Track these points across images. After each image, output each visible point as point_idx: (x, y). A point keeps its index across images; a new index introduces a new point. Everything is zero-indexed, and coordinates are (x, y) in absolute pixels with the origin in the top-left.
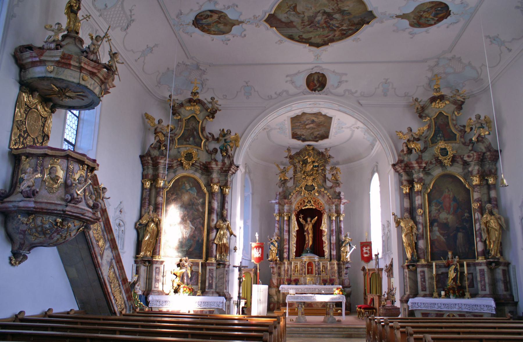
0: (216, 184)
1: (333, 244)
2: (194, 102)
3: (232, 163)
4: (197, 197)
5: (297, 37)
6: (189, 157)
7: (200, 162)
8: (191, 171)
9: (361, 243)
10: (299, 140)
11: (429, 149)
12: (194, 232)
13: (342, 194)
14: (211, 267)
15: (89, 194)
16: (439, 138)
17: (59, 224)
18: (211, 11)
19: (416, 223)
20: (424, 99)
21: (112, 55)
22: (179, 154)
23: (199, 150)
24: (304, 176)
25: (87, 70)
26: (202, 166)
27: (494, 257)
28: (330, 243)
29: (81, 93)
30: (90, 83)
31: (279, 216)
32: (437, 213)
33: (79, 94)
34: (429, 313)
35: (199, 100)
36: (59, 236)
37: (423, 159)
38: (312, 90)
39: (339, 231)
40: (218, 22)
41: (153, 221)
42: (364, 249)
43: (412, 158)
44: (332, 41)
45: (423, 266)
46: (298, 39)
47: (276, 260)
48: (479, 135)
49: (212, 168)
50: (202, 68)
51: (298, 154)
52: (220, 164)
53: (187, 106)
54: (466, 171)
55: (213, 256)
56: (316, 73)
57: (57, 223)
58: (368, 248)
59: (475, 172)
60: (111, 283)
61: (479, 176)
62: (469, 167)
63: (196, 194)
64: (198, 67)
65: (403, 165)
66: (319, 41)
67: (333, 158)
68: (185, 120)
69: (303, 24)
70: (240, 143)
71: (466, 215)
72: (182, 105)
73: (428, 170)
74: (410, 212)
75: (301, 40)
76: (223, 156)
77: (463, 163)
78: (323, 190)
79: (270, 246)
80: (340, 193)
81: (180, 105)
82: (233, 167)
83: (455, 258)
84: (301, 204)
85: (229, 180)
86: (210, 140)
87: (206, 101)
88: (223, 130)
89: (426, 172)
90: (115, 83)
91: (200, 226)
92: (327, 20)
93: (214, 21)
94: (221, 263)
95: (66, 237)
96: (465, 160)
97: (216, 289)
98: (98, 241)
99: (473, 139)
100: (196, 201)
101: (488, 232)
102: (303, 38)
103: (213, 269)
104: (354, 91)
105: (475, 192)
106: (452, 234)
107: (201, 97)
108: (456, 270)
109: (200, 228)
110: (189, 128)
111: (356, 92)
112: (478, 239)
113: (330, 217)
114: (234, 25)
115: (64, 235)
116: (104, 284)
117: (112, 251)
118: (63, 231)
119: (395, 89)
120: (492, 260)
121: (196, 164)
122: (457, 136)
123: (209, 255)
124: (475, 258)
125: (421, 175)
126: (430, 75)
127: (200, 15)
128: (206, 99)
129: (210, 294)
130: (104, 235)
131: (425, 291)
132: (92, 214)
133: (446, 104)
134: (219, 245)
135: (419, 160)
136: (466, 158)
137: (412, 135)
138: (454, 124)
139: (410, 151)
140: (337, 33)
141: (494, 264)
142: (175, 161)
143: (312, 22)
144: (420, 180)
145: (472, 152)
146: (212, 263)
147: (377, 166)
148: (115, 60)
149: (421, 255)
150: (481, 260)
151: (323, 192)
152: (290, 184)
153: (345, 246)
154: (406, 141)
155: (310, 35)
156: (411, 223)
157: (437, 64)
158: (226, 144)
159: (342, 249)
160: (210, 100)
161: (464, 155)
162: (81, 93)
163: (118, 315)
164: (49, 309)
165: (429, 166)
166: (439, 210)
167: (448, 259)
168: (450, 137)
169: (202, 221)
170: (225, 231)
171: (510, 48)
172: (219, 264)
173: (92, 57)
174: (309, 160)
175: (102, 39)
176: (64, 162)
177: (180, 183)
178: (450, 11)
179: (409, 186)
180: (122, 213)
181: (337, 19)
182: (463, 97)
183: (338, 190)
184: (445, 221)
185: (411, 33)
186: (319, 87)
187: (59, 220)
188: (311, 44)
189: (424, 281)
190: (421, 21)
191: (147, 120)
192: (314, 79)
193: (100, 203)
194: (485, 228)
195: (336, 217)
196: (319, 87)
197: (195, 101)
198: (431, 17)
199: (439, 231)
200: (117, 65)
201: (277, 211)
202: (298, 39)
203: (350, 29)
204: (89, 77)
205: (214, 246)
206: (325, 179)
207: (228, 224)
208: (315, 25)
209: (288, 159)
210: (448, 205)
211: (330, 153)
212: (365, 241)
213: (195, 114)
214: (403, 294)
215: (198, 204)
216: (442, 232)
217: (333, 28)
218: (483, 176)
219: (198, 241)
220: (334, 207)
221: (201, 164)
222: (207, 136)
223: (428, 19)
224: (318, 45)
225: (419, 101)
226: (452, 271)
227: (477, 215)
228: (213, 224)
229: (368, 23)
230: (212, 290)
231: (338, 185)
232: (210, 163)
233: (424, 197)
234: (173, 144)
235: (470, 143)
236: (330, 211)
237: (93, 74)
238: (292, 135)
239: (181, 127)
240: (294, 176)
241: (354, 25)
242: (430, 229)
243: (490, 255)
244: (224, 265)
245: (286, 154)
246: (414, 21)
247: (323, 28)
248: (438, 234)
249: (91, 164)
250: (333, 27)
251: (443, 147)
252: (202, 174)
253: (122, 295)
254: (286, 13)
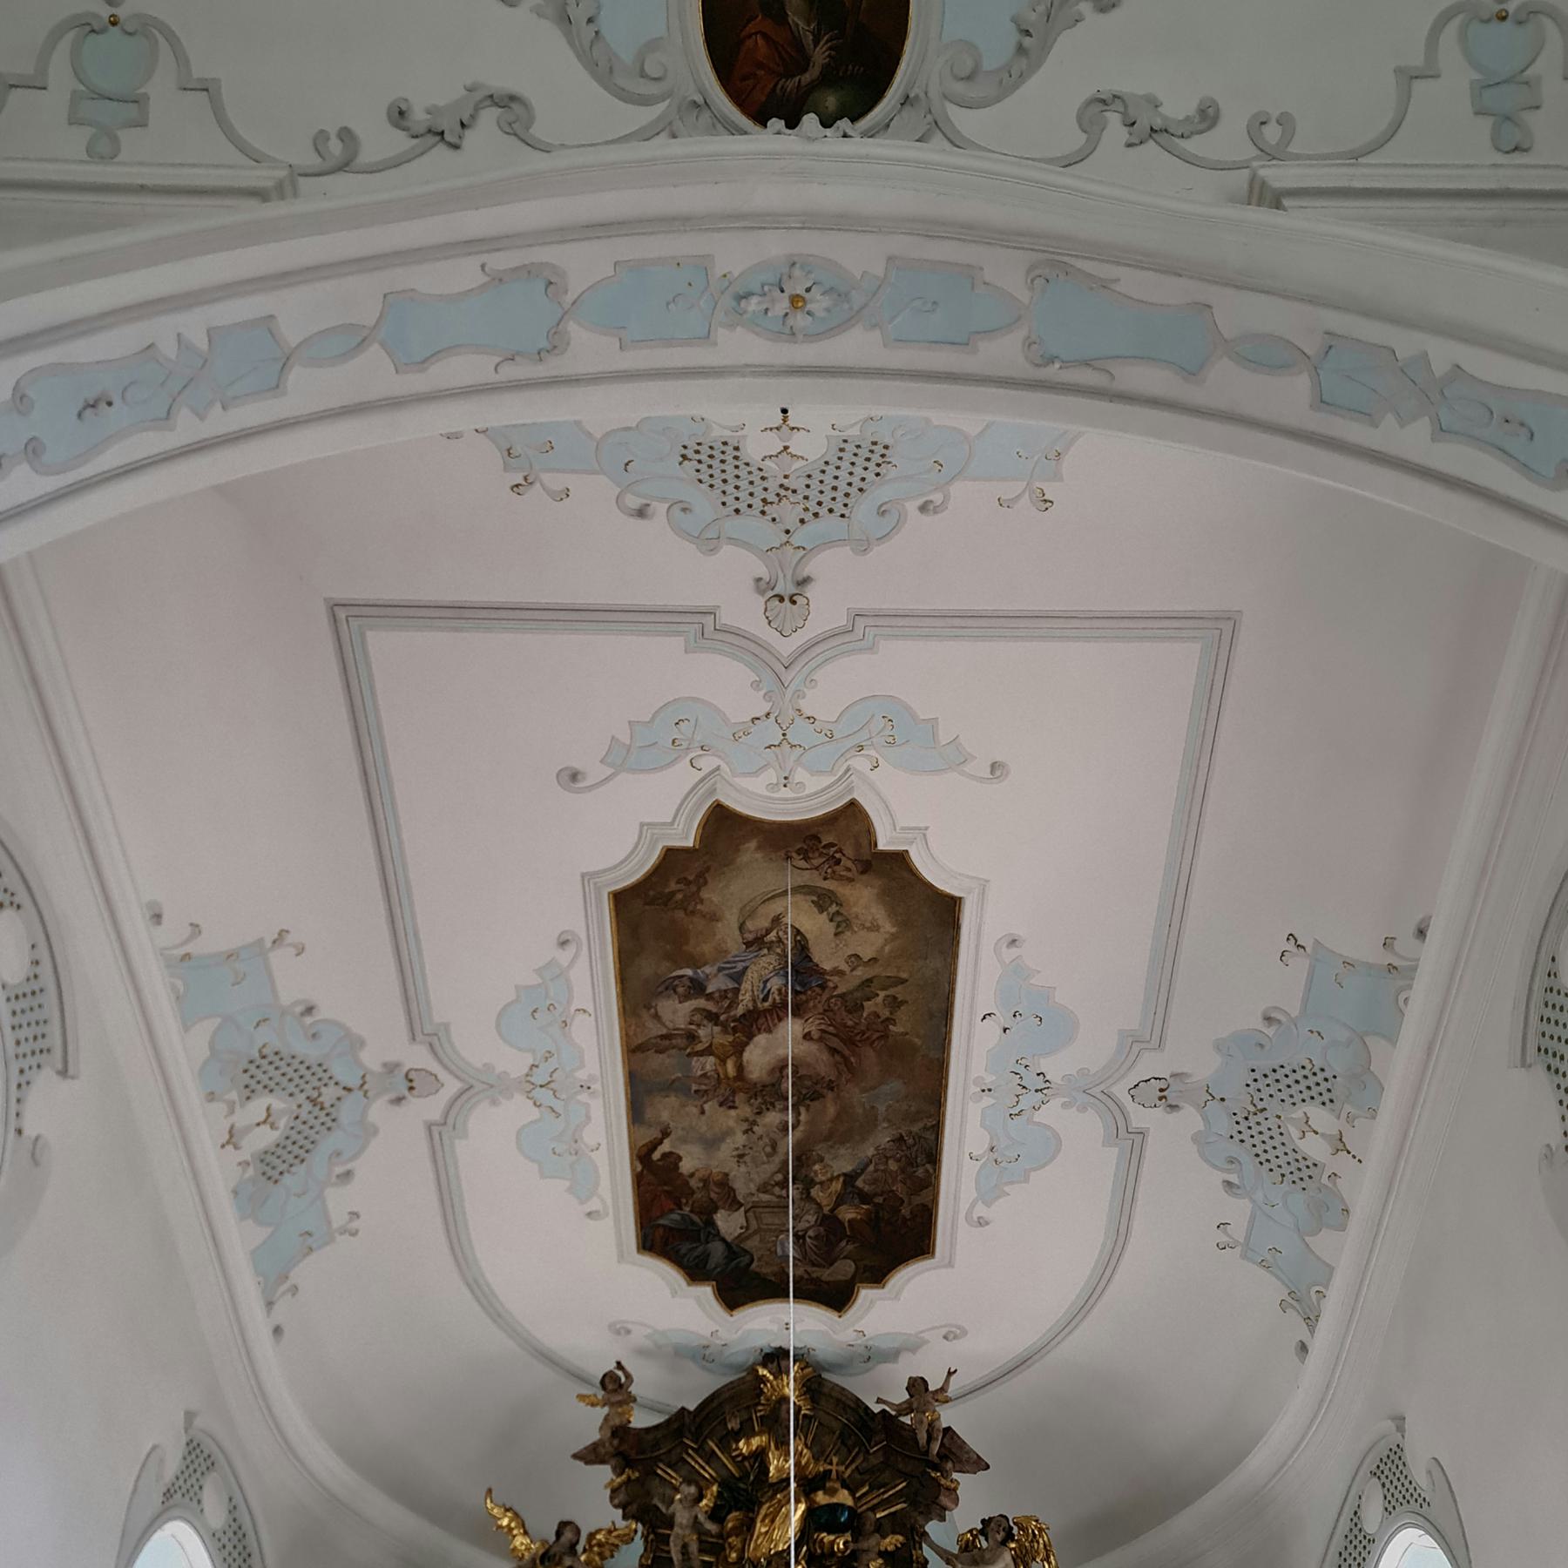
104: (1177, 108)
186: (828, 79)
196: (828, 79)
245: (590, 1424)
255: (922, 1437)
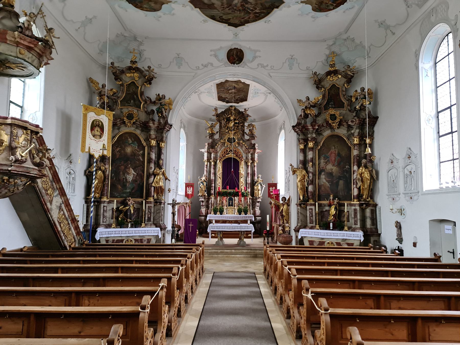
0: (154, 139)
1: (248, 184)
2: (133, 70)
3: (166, 123)
4: (138, 150)
5: (218, 17)
6: (130, 117)
7: (140, 121)
8: (133, 129)
9: (269, 184)
10: (224, 102)
11: (322, 114)
12: (136, 177)
13: (256, 145)
14: (150, 205)
15: (36, 152)
16: (330, 106)
17: (5, 181)
19: (308, 172)
20: (322, 71)
21: (48, 31)
22: (122, 114)
23: (138, 111)
24: (227, 131)
25: (23, 45)
26: (141, 124)
27: (365, 200)
28: (246, 183)
29: (20, 65)
30: (28, 57)
31: (208, 162)
32: (325, 165)
33: (19, 65)
34: (314, 241)
35: (138, 68)
36: (6, 191)
37: (317, 122)
38: (232, 63)
39: (253, 175)
41: (100, 169)
42: (271, 188)
43: (309, 120)
44: (248, 22)
45: (311, 205)
46: (219, 19)
47: (205, 196)
48: (362, 105)
49: (150, 126)
50: (139, 40)
51: (222, 113)
52: (156, 123)
53: (128, 73)
54: (350, 132)
55: (152, 196)
56: (235, 48)
57: (4, 180)
58: (274, 188)
59: (356, 134)
60: (61, 223)
61: (359, 137)
62: (352, 130)
63: (137, 147)
64: (135, 39)
65: (300, 127)
66: (237, 22)
67: (251, 116)
68: (126, 85)
69: (223, 6)
70: (173, 107)
71: (347, 167)
72: (122, 72)
73: (320, 131)
74: (304, 163)
75: (222, 20)
76: (159, 116)
77: (348, 126)
78: (241, 142)
79: (200, 184)
80: (254, 144)
81: (121, 71)
82: (167, 126)
83: (335, 200)
84: (224, 153)
85: (165, 136)
86: (148, 103)
87: (143, 69)
88: (159, 95)
89: (318, 132)
90: (52, 56)
91: (141, 172)
92: (242, 3)
94: (158, 201)
95: (13, 190)
96: (349, 124)
97: (153, 222)
98: (46, 190)
99: (357, 107)
100: (137, 152)
101: (362, 181)
102: (223, 19)
103: (151, 206)
104: (265, 65)
105: (355, 149)
106: (335, 182)
107: (139, 65)
108: (336, 208)
109: (141, 174)
110: (130, 92)
111: (267, 66)
112: (355, 186)
113: (246, 163)
114: (164, 4)
115: (12, 190)
116: (54, 225)
117: (61, 197)
118: (10, 186)
119: (299, 64)
120: (363, 202)
121: (137, 123)
122: (345, 105)
123: (148, 195)
124: (352, 200)
125: (314, 135)
126: (327, 52)
128: (143, 68)
129: (149, 225)
130: (53, 185)
131: (313, 223)
132: (37, 171)
133: (338, 77)
134: (157, 187)
135: (314, 123)
136: (350, 123)
137: (309, 103)
138: (343, 94)
139: (306, 116)
140: (252, 16)
141: (364, 205)
142: (118, 120)
143: (230, 5)
144: (313, 139)
145: (356, 118)
146: (151, 202)
147: (284, 124)
148: (51, 35)
149: (310, 197)
150: (356, 202)
151: (242, 143)
152: (217, 137)
153: (257, 186)
154: (304, 108)
155: (230, 17)
156: (304, 172)
157: (334, 44)
158: (161, 107)
159: (255, 188)
160: (147, 69)
161: (348, 121)
162: (20, 65)
163: (68, 248)
164: (3, 249)
165: (321, 128)
166: (326, 163)
167: (330, 199)
168: (340, 105)
169: (142, 169)
170: (161, 176)
171: (394, 32)
172: (156, 202)
173: (27, 33)
174: (232, 118)
175: (36, 16)
176: (8, 129)
177: (123, 138)
179: (304, 144)
180: (72, 164)
181: (251, 3)
182: (352, 72)
183: (253, 142)
184: (330, 171)
185: (313, 17)
187: (6, 178)
188: (230, 24)
189: (312, 216)
190: (321, 6)
191: (91, 84)
192: (233, 53)
193: (45, 162)
194: (360, 178)
195: (252, 163)
196: (237, 60)
197: (134, 69)
198: (330, 3)
199: (325, 179)
200: (54, 40)
201: (206, 158)
202: (219, 19)
203: (262, 13)
204: (26, 51)
205: (153, 188)
206: (244, 133)
207: (164, 171)
208: (233, 8)
209: (215, 117)
210: (333, 159)
211: (248, 113)
212: (271, 183)
213: (135, 80)
214: (296, 225)
215: (139, 155)
216: (327, 179)
217: (248, 11)
218: (362, 137)
219: (139, 184)
220: (250, 156)
221: (141, 122)
222: (145, 99)
223: (328, 5)
224: (236, 26)
225: (317, 74)
226: (333, 209)
227: (355, 168)
228: (151, 171)
229: (277, 7)
230: (150, 223)
231: (253, 138)
232: (148, 122)
233: (315, 152)
234: (116, 105)
235: (355, 110)
236: (246, 158)
237: (29, 49)
238: (218, 97)
239: (122, 91)
240: (219, 130)
241: (266, 8)
242: (318, 177)
243: (362, 198)
244: (161, 203)
245: (214, 113)
246: (316, 6)
247: (240, 10)
248: (324, 181)
249: (34, 129)
250: (248, 10)
251: (333, 113)
252: (142, 131)
253: (72, 231)
255: (245, 115)
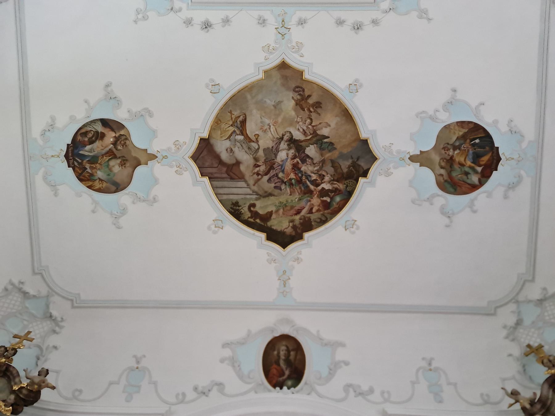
18: (105, 123)
38: (274, 386)
40: (111, 154)
46: (247, 215)
92: (295, 161)
93: (104, 152)
104: (365, 388)
111: (371, 391)
127: (83, 131)
178: (498, 148)
186: (289, 378)
196: (289, 378)
203: (336, 191)
229: (365, 174)
254: (229, 138)
